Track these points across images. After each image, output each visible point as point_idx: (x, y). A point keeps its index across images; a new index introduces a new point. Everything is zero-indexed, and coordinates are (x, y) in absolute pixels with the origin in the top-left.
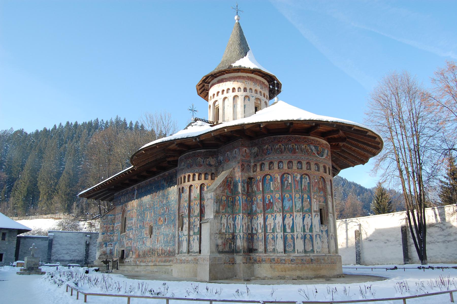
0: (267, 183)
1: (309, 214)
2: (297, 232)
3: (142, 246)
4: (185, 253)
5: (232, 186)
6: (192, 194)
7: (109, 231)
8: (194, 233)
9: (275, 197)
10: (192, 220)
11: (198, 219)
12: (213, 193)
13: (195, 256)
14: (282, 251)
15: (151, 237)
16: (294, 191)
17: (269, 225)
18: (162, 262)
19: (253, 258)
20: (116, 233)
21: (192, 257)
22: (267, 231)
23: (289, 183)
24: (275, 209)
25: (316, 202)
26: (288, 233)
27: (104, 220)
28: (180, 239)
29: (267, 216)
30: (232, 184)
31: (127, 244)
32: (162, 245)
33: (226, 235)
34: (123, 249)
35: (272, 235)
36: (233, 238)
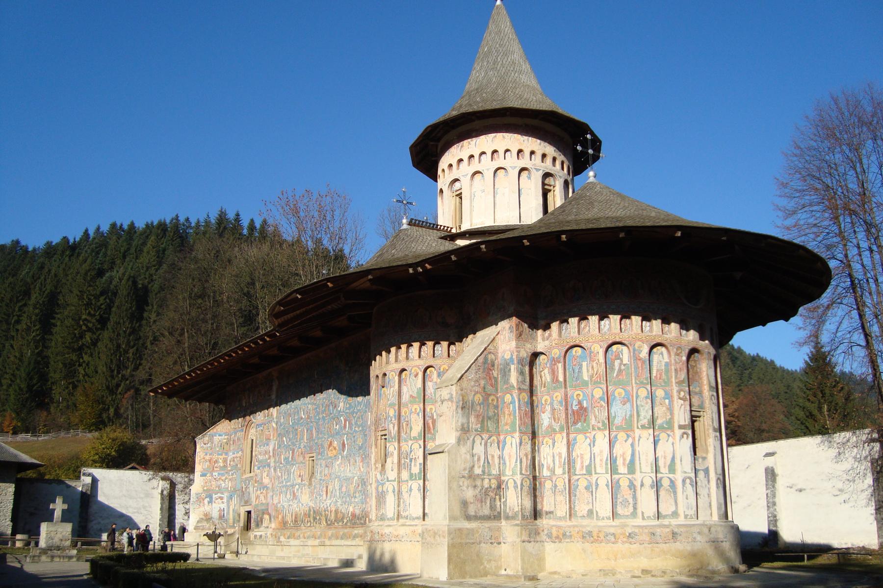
0: (575, 365)
1: (668, 433)
2: (641, 472)
3: (291, 503)
4: (392, 519)
5: (496, 372)
6: (404, 389)
7: (215, 469)
8: (411, 475)
9: (592, 395)
10: (405, 447)
11: (420, 445)
12: (454, 387)
13: (412, 525)
14: (608, 515)
15: (310, 484)
16: (636, 383)
17: (579, 458)
18: (337, 538)
19: (543, 531)
20: (232, 474)
21: (407, 528)
22: (575, 470)
23: (624, 365)
24: (593, 422)
25: (683, 407)
26: (621, 476)
27: (205, 444)
28: (380, 489)
29: (575, 439)
30: (496, 367)
31: (257, 497)
32: (337, 501)
33: (483, 480)
34: (248, 508)
35: (586, 481)
36: (499, 487)
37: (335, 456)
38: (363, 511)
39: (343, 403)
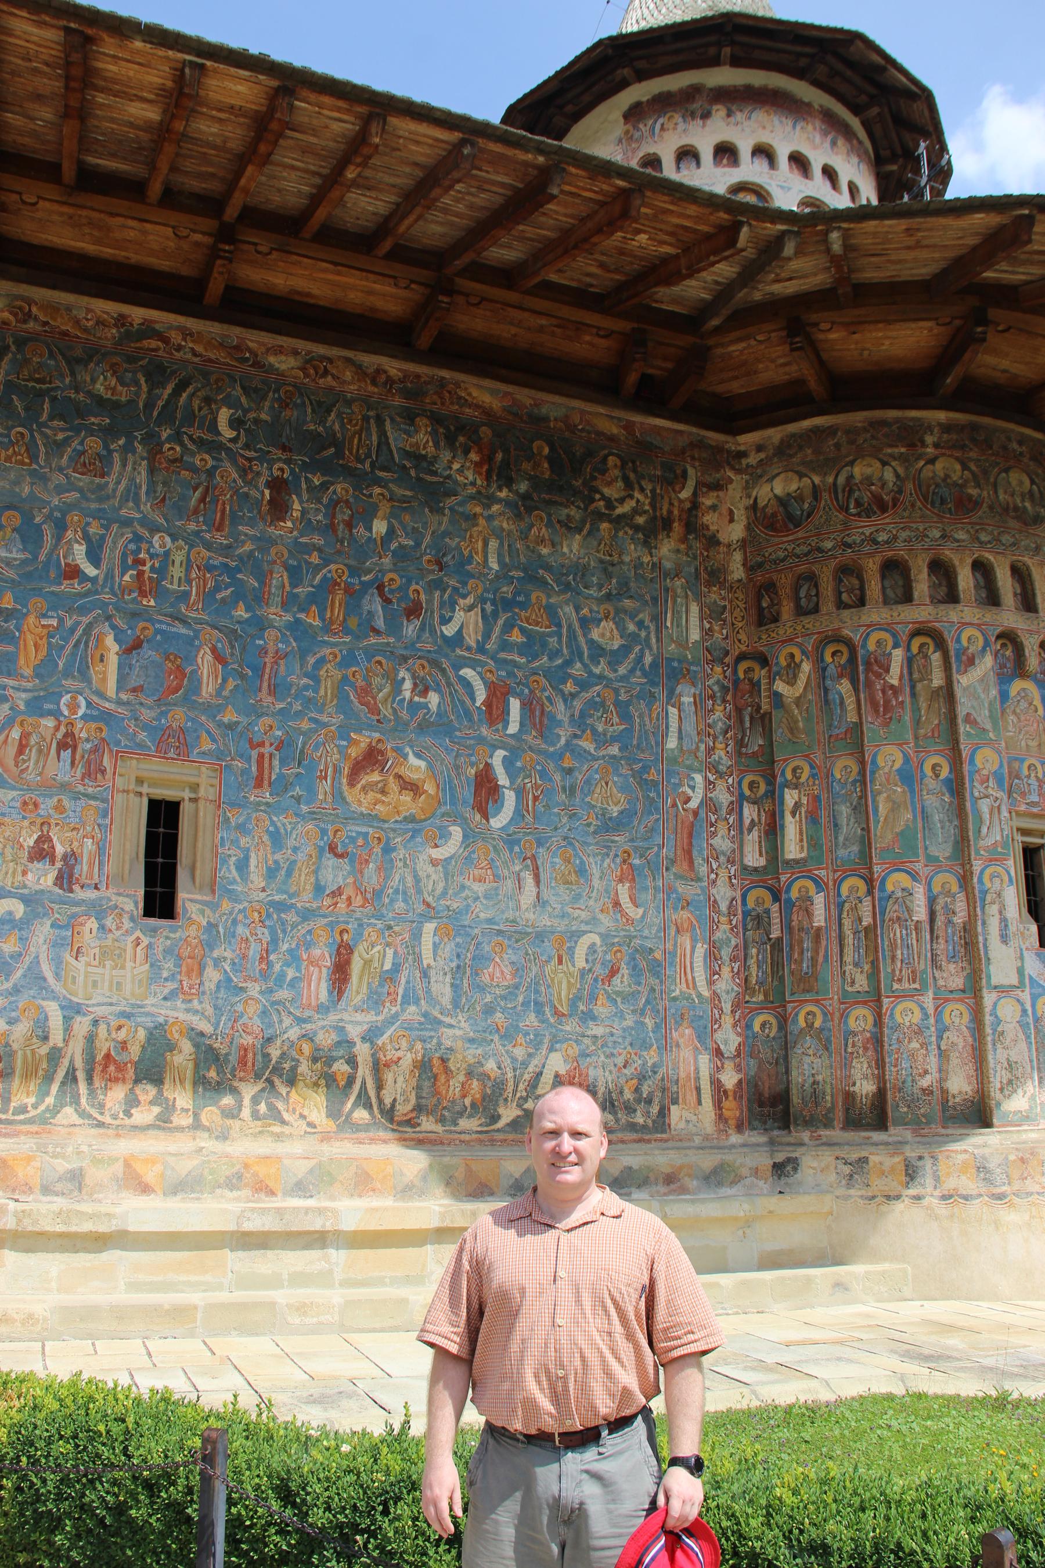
37: (411, 819)
38: (642, 1078)
39: (475, 617)
